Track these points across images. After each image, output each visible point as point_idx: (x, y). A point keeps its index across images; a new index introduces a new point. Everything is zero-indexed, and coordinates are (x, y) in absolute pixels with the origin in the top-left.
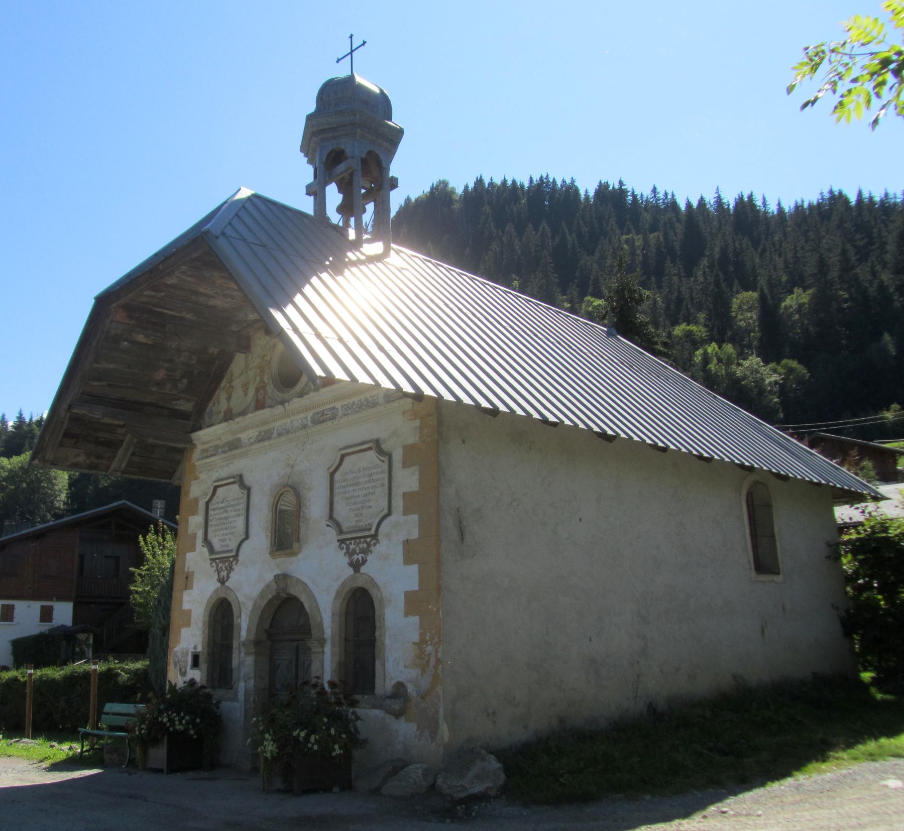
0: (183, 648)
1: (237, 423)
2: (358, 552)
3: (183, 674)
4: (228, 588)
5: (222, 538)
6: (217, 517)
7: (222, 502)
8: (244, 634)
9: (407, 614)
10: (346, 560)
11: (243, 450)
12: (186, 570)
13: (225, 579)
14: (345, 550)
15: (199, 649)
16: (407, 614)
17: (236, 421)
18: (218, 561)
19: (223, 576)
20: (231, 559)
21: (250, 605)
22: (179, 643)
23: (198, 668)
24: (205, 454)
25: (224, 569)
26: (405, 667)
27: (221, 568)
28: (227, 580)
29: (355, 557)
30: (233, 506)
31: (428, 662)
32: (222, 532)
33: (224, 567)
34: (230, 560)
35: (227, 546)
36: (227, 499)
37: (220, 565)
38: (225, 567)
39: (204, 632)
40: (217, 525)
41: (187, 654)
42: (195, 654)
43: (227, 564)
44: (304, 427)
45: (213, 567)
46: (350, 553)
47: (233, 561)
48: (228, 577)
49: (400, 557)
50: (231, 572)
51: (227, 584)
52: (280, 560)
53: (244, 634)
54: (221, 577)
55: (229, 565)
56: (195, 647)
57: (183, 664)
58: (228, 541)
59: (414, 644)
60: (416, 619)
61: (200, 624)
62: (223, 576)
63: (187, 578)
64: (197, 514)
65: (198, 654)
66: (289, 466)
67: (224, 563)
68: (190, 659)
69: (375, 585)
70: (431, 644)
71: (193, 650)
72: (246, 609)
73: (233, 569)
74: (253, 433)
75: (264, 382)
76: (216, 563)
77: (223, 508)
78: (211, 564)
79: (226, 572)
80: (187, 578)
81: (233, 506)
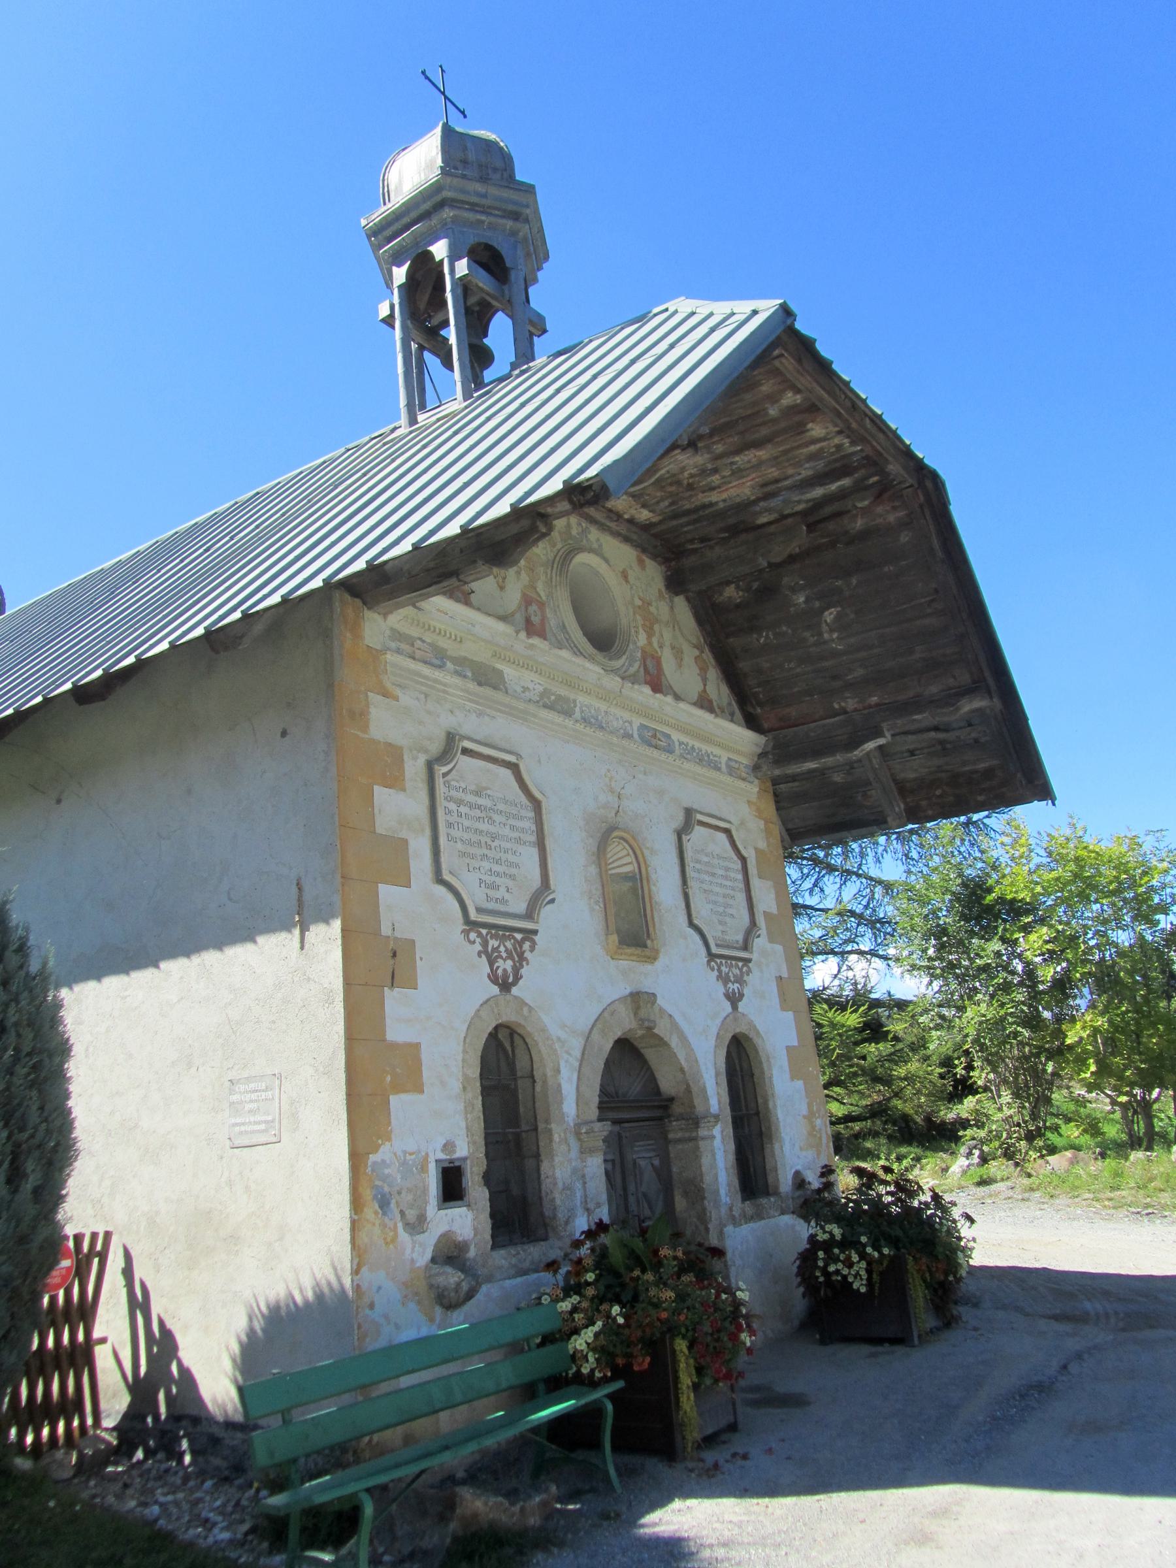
0: (405, 1152)
1: (532, 647)
2: (732, 979)
3: (417, 1225)
4: (522, 1003)
5: (489, 879)
6: (467, 823)
7: (478, 793)
8: (569, 1107)
9: (792, 1079)
10: (720, 989)
11: (499, 696)
12: (386, 930)
13: (511, 980)
14: (716, 973)
15: (462, 1150)
16: (792, 1079)
17: (531, 641)
18: (484, 932)
19: (505, 970)
20: (519, 936)
21: (577, 1045)
22: (389, 1139)
23: (459, 1203)
24: (404, 647)
25: (504, 955)
26: (801, 1149)
27: (495, 949)
28: (515, 983)
29: (730, 985)
30: (509, 816)
31: (820, 1138)
32: (486, 865)
33: (502, 949)
34: (514, 938)
35: (503, 901)
36: (489, 792)
37: (493, 943)
38: (507, 950)
39: (469, 1106)
40: (470, 843)
41: (423, 1168)
42: (446, 1165)
43: (509, 944)
44: (628, 736)
45: (474, 942)
46: (724, 979)
47: (523, 940)
48: (517, 978)
49: (775, 1000)
50: (522, 967)
51: (515, 991)
52: (624, 964)
53: (569, 1107)
54: (500, 972)
55: (515, 949)
56: (448, 1146)
57: (407, 1197)
58: (503, 890)
59: (805, 1117)
60: (799, 1084)
61: (455, 1085)
62: (505, 970)
63: (394, 955)
64: (404, 790)
65: (457, 1164)
66: (612, 791)
67: (503, 939)
68: (433, 1183)
69: (758, 1033)
70: (819, 1117)
71: (441, 1156)
72: (567, 1052)
73: (526, 959)
74: (534, 683)
75: (540, 596)
76: (480, 935)
77: (479, 807)
78: (466, 933)
79: (509, 963)
80: (394, 955)
81: (509, 816)
